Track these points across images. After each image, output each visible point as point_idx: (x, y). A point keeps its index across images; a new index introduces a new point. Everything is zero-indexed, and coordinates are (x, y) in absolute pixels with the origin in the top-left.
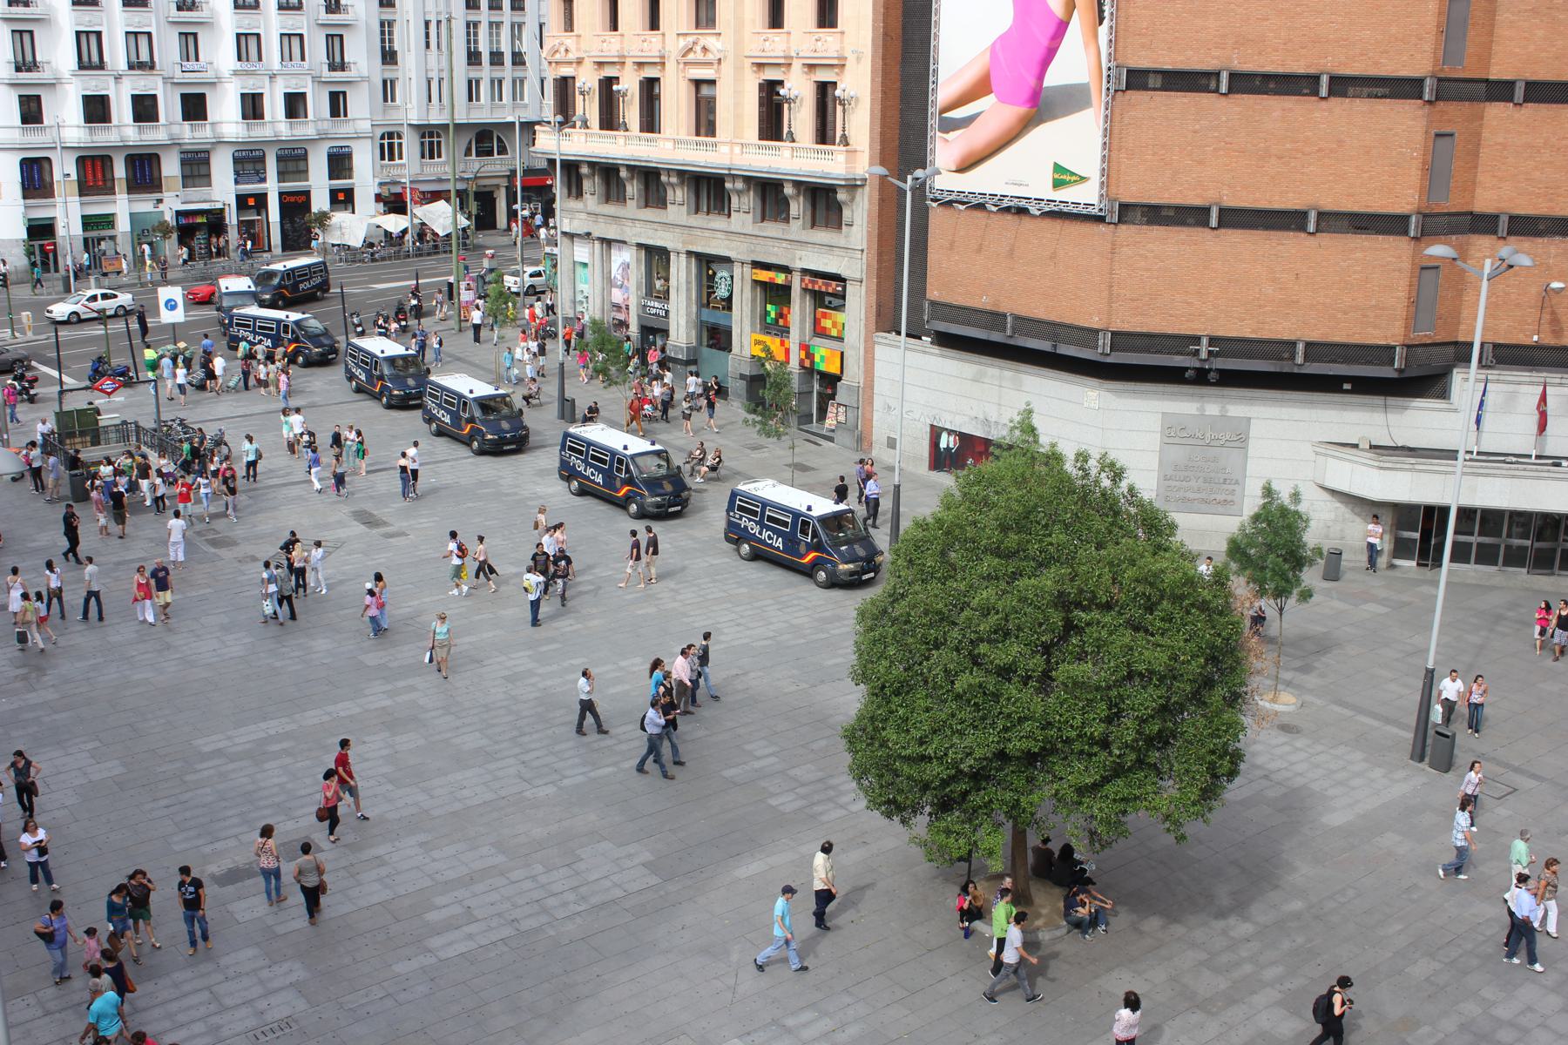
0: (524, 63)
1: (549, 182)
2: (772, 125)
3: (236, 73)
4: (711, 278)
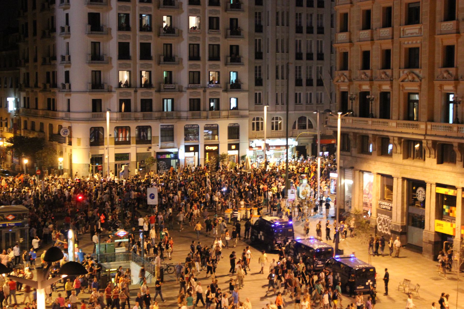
1: (333, 142)
3: (188, 88)
4: (415, 191)
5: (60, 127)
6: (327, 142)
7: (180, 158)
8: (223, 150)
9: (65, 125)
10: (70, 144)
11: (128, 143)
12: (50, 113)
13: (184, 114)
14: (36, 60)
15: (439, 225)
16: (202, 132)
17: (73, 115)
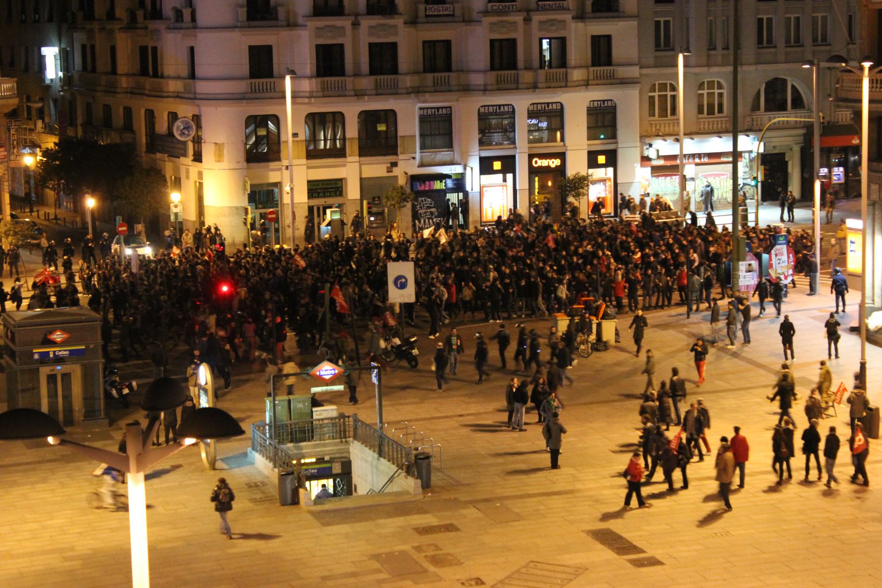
1: (855, 141)
5: (173, 117)
6: (838, 141)
7: (468, 188)
8: (576, 166)
9: (185, 111)
10: (198, 158)
11: (339, 153)
12: (148, 83)
13: (478, 79)
16: (522, 123)
17: (203, 87)
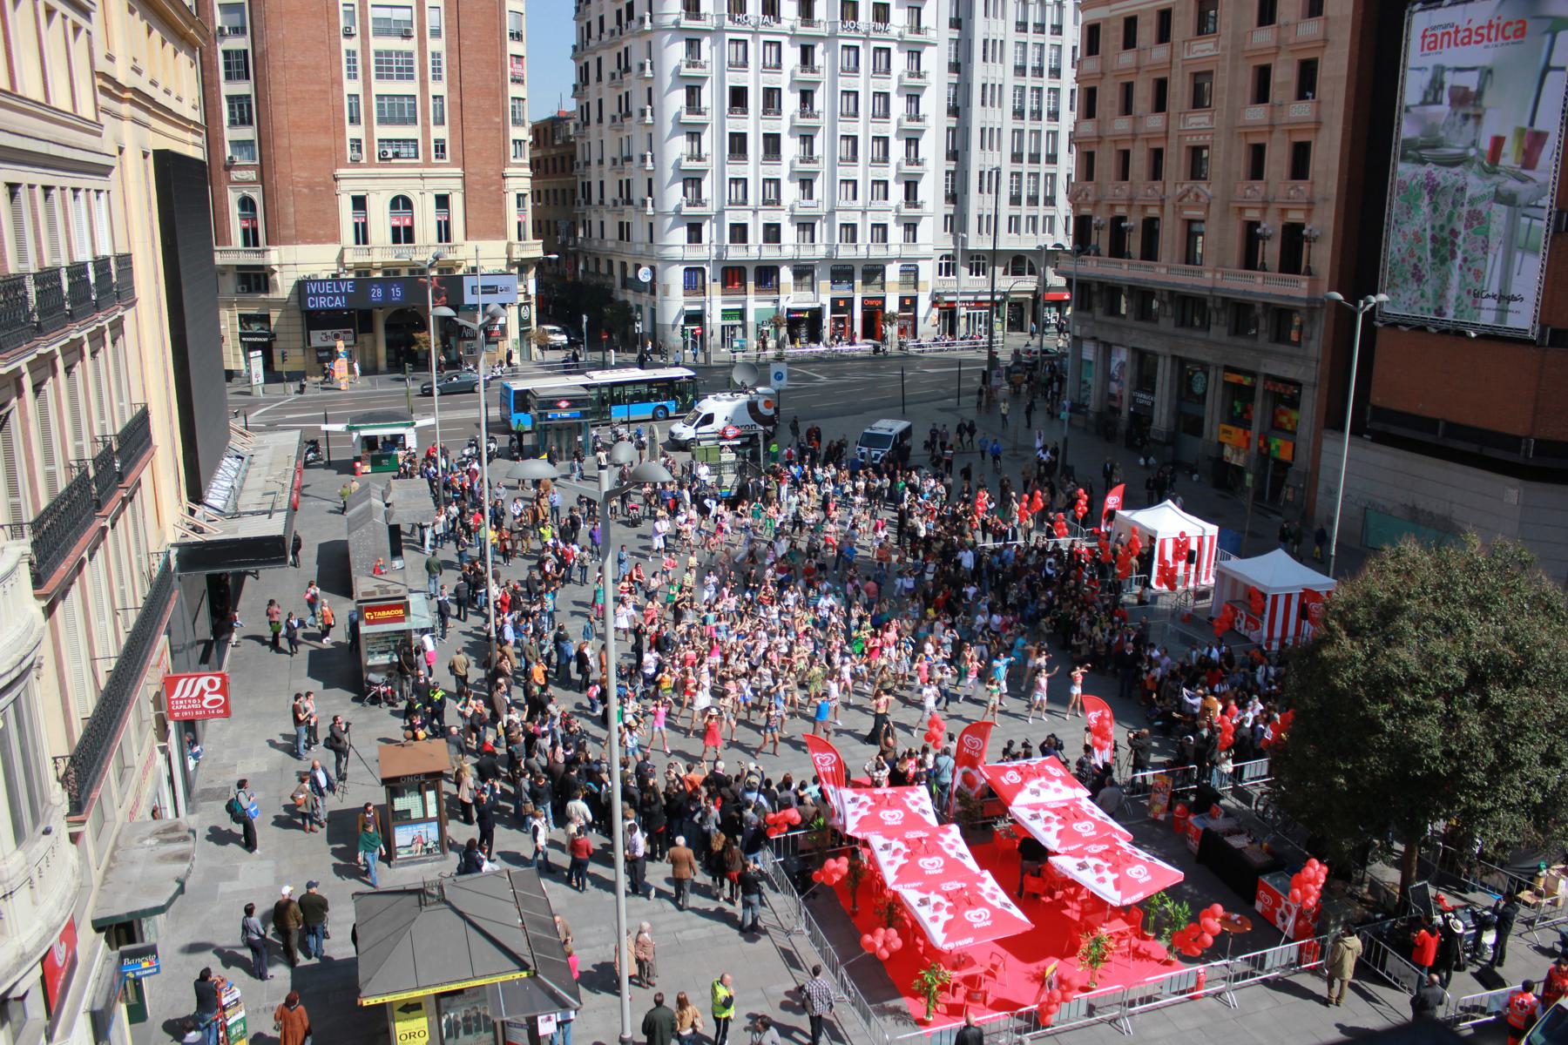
0: (1053, 204)
2: (1250, 260)
14: (601, 162)
15: (1225, 431)
